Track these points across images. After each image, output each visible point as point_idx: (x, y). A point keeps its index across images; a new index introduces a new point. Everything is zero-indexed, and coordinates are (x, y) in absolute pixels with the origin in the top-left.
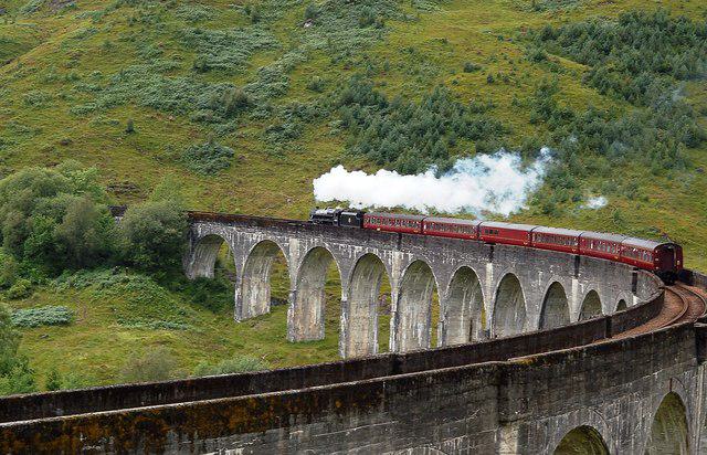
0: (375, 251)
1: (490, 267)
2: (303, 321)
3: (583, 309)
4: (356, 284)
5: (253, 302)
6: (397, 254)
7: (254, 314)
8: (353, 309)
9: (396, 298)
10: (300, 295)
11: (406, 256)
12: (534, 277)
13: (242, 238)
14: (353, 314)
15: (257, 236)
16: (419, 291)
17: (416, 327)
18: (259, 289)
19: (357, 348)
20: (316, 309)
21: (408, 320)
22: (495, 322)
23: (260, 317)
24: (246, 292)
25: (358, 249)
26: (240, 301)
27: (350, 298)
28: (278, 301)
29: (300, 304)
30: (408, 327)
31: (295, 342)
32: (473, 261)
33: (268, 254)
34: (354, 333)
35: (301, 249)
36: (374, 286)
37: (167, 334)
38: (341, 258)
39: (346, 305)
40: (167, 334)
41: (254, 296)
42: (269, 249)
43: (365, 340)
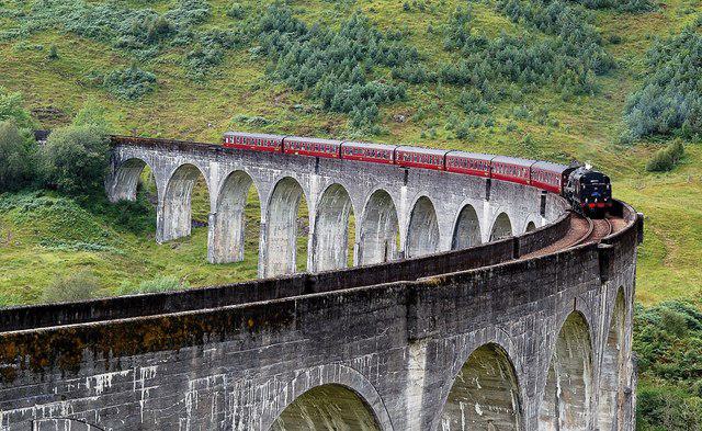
0: (294, 175)
1: (404, 189)
2: (223, 243)
3: (494, 230)
4: (275, 207)
5: (175, 225)
7: (175, 236)
8: (272, 231)
10: (220, 217)
15: (179, 159)
16: (337, 214)
20: (235, 229)
22: (408, 243)
23: (181, 239)
24: (167, 214)
26: (162, 224)
27: (269, 220)
28: (199, 224)
29: (220, 226)
31: (215, 264)
33: (189, 177)
34: (273, 255)
36: (292, 209)
37: (89, 255)
39: (266, 228)
40: (89, 255)
41: (175, 218)
42: (190, 172)
43: (284, 261)
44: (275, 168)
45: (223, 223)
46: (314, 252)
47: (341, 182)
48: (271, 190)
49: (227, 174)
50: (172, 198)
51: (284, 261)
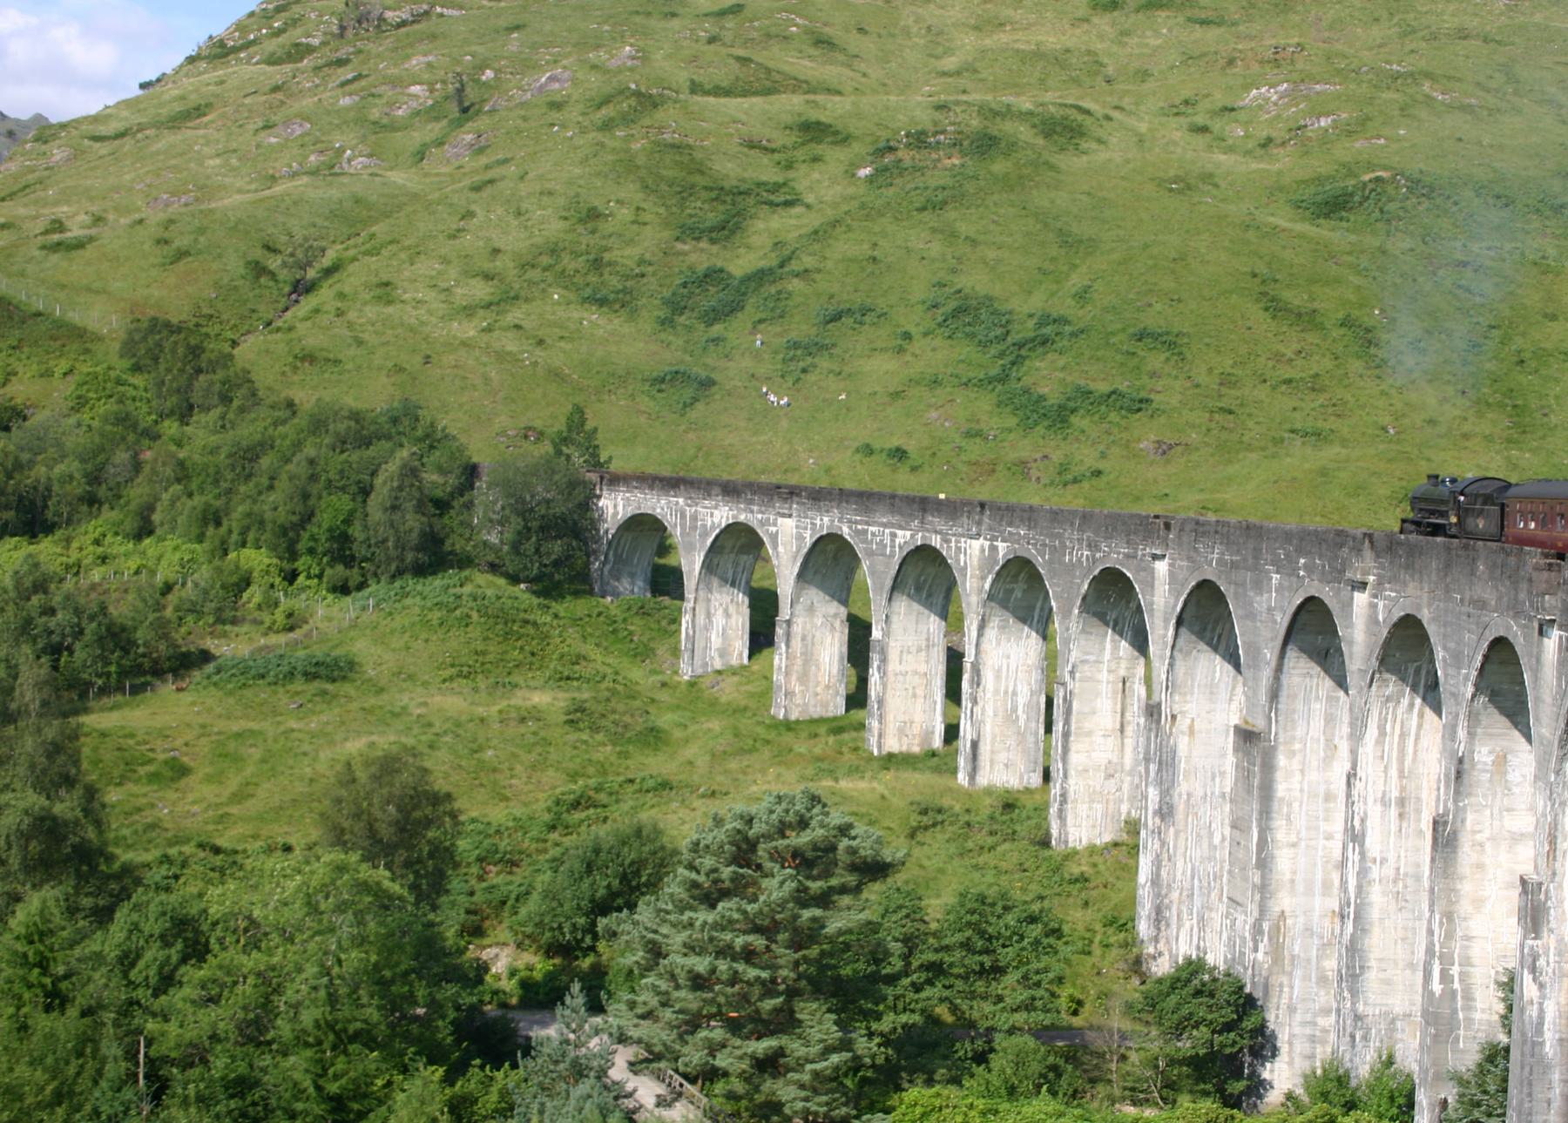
0: (936, 541)
2: (804, 678)
5: (716, 641)
6: (976, 545)
8: (893, 654)
9: (974, 634)
10: (797, 629)
11: (993, 549)
12: (1260, 585)
13: (694, 518)
14: (893, 666)
15: (719, 514)
17: (1015, 693)
18: (727, 615)
19: (901, 732)
20: (831, 648)
21: (998, 677)
24: (701, 619)
25: (903, 536)
26: (692, 640)
29: (796, 644)
30: (997, 692)
32: (1127, 556)
35: (800, 538)
38: (870, 554)
43: (919, 717)
44: (901, 528)
45: (804, 639)
46: (975, 702)
47: (1032, 553)
48: (893, 572)
49: (809, 542)
50: (710, 591)
51: (919, 717)
